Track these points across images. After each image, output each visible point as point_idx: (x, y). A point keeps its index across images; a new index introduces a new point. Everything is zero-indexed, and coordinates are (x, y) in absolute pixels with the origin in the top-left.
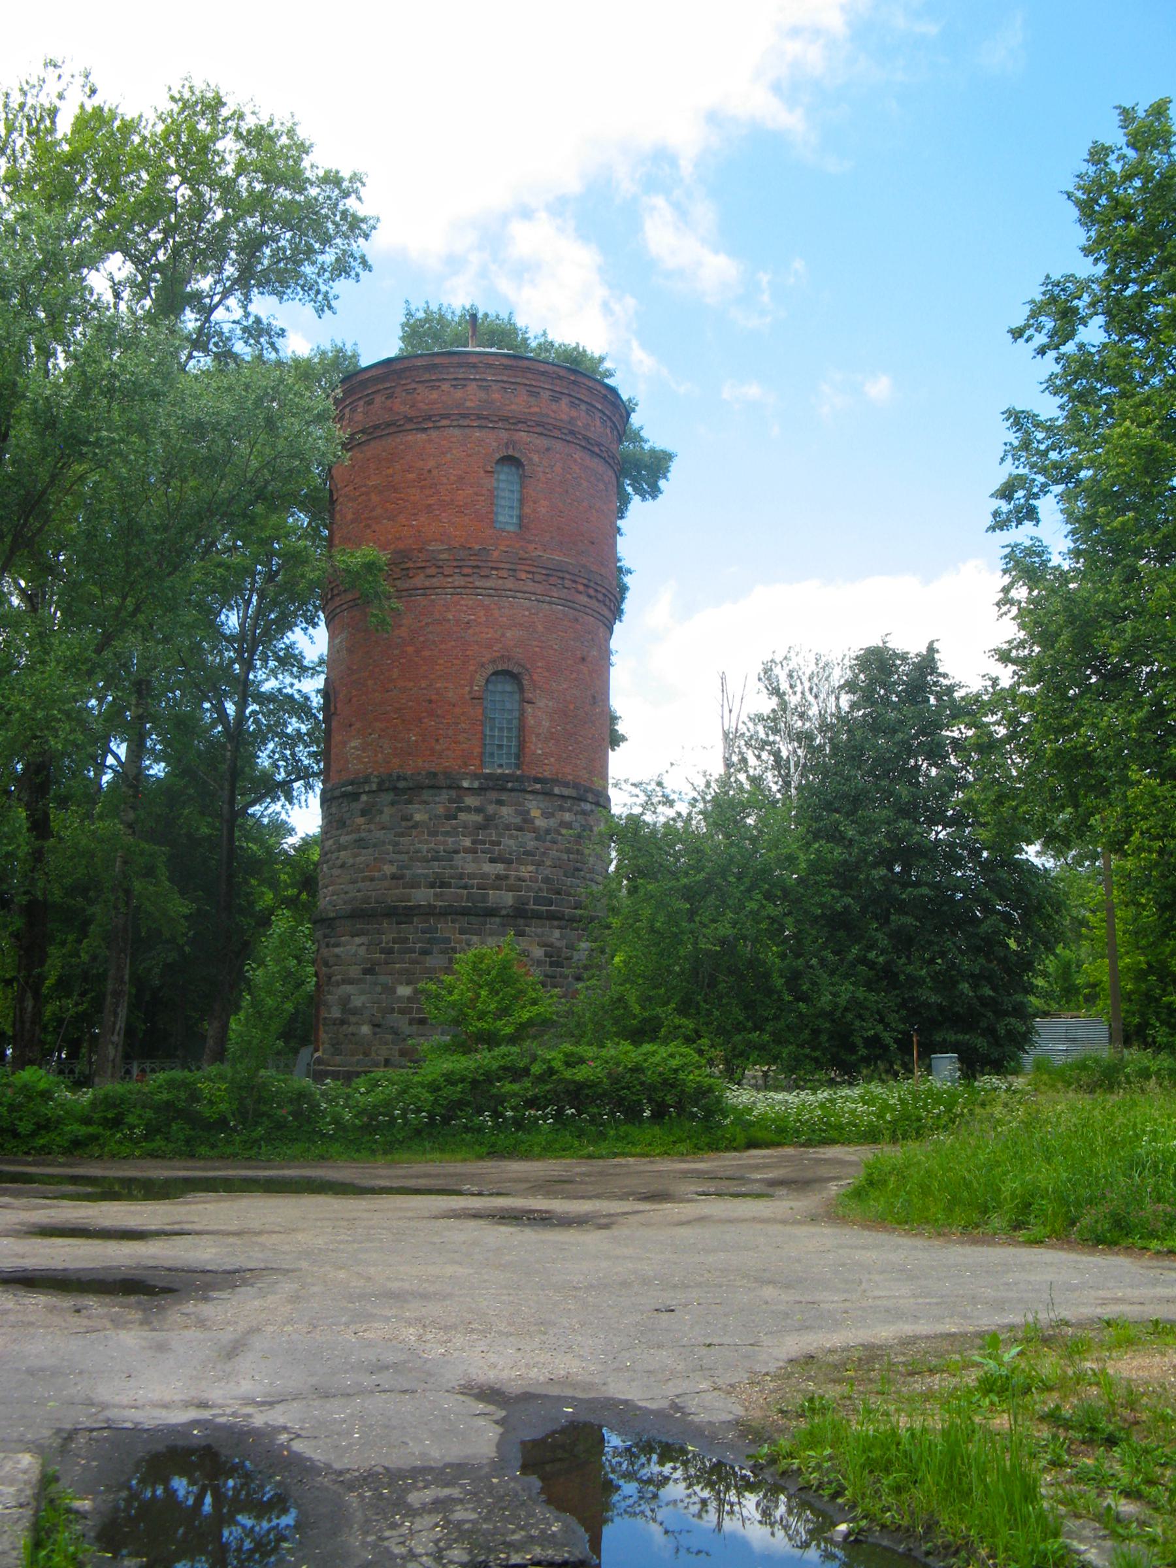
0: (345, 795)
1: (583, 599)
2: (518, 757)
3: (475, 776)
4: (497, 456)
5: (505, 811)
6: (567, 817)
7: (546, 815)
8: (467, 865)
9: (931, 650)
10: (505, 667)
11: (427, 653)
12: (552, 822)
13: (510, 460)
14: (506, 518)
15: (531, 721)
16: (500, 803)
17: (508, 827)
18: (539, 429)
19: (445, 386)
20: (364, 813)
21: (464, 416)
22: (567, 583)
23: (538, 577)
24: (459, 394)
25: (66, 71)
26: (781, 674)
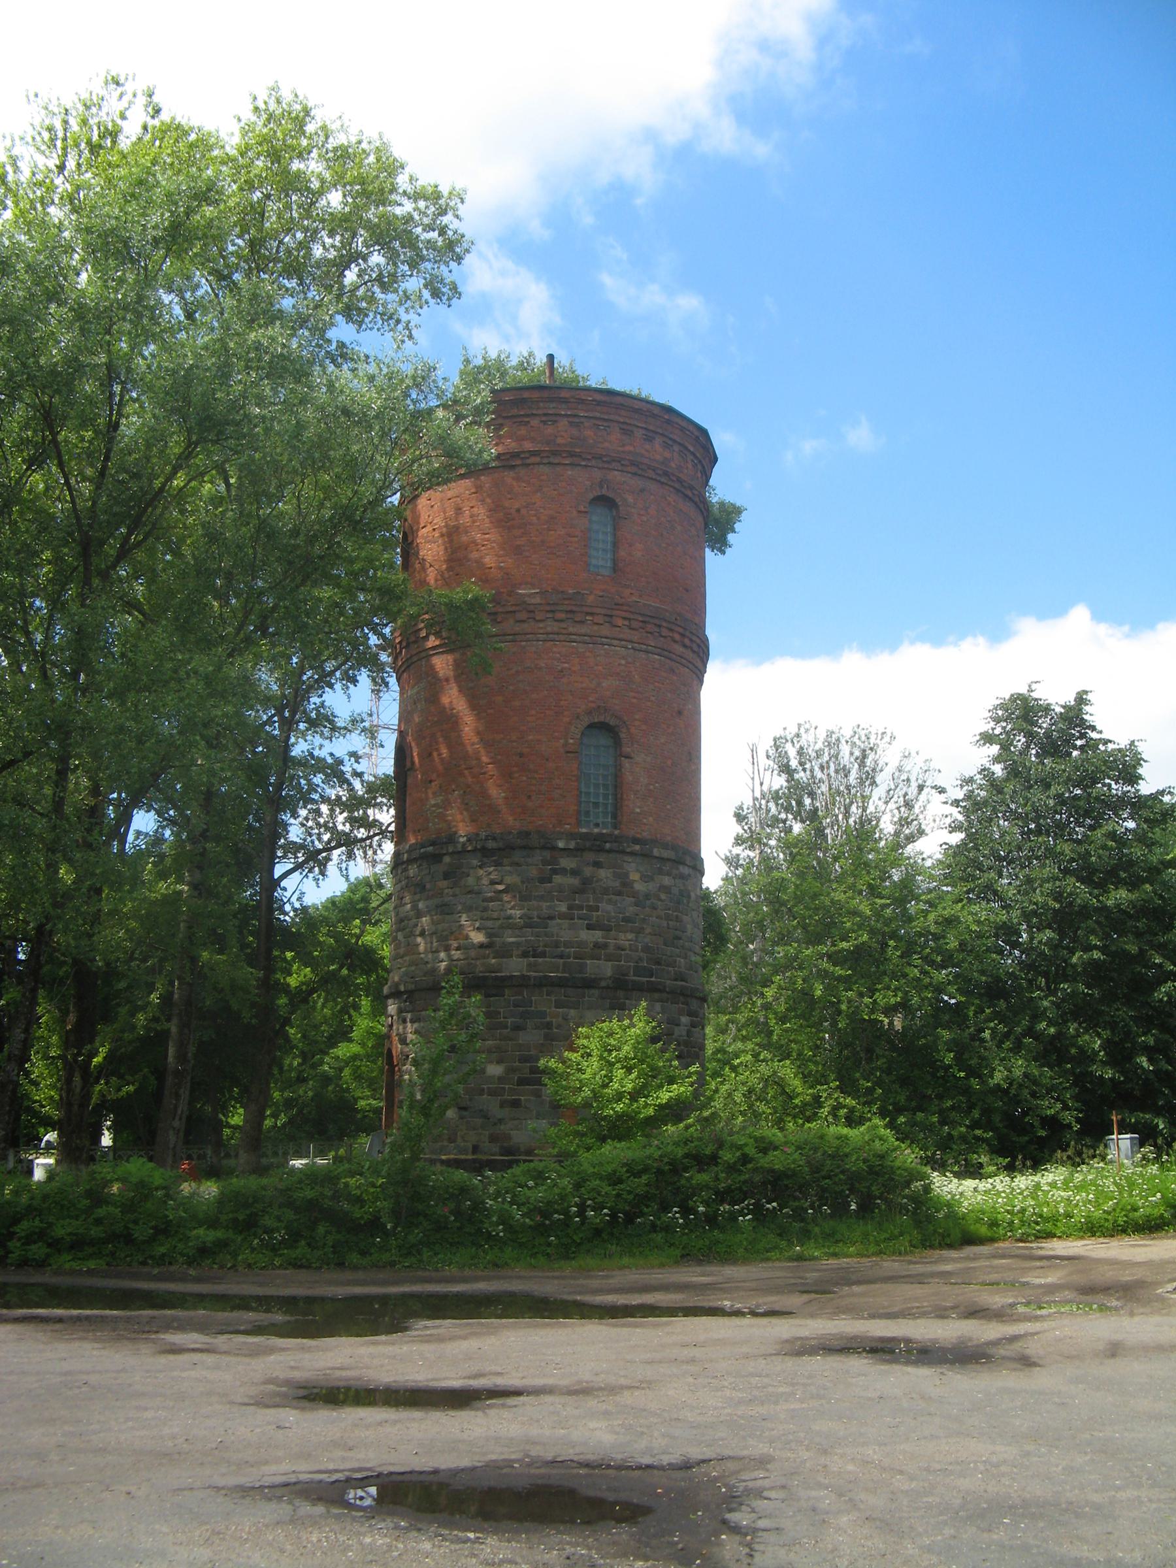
0: (424, 857)
1: (679, 649)
2: (615, 816)
3: (571, 836)
4: (591, 496)
5: (603, 873)
6: (667, 881)
7: (645, 878)
8: (562, 931)
9: (1081, 699)
10: (602, 719)
11: (517, 703)
12: (652, 887)
13: (606, 502)
14: (601, 560)
15: (629, 778)
16: (597, 865)
17: (606, 891)
18: (633, 469)
19: (535, 422)
20: (446, 876)
21: (555, 453)
22: (665, 632)
23: (635, 624)
24: (549, 430)
25: (129, 87)
26: (792, 752)
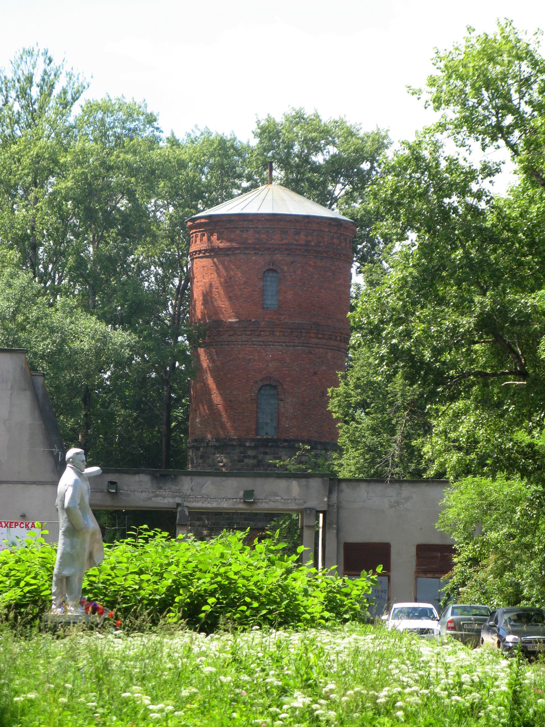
3: (253, 440)
4: (264, 270)
10: (268, 383)
11: (229, 376)
16: (265, 453)
18: (287, 252)
21: (246, 248)
